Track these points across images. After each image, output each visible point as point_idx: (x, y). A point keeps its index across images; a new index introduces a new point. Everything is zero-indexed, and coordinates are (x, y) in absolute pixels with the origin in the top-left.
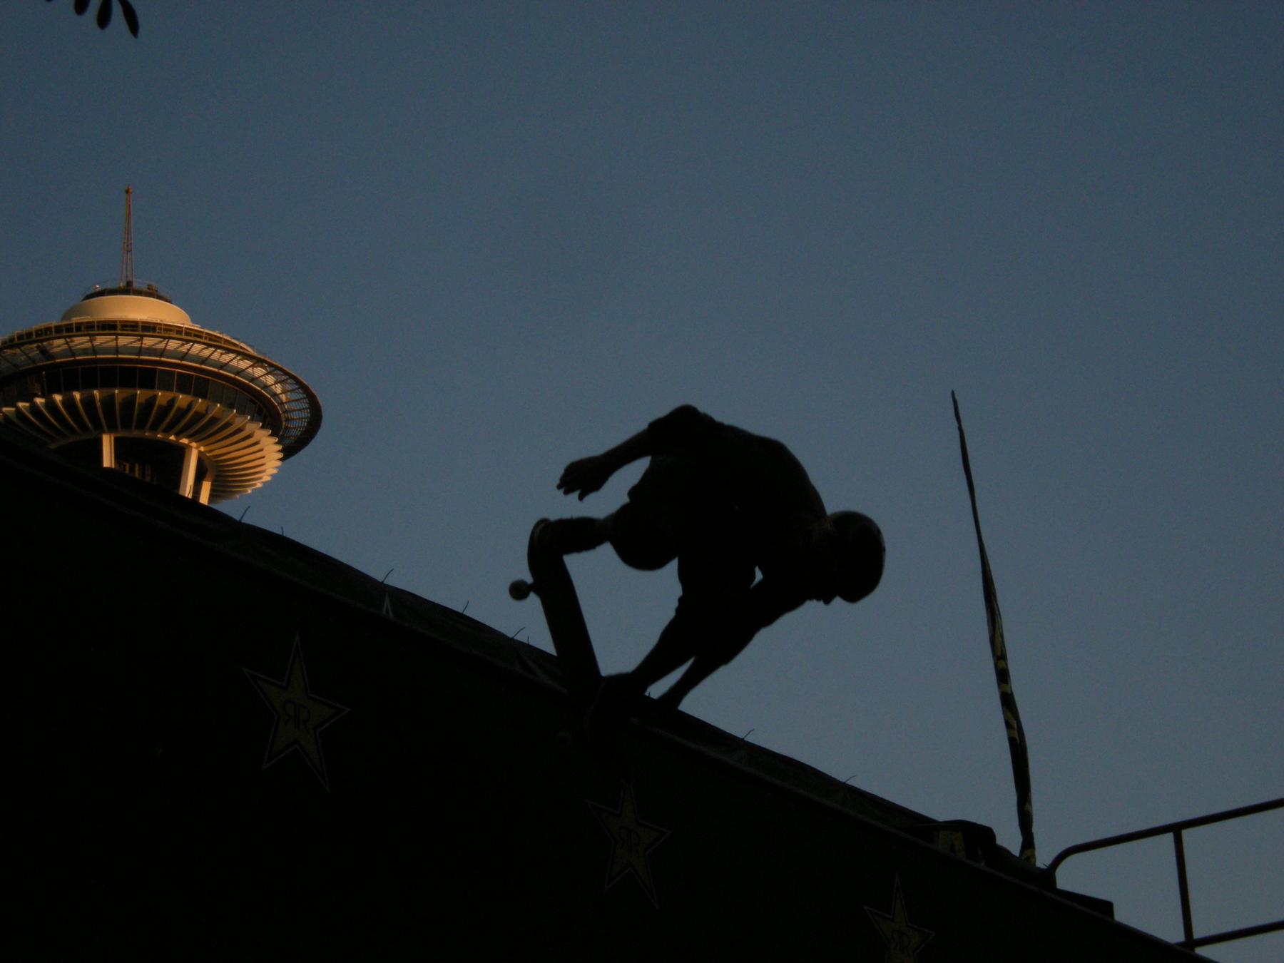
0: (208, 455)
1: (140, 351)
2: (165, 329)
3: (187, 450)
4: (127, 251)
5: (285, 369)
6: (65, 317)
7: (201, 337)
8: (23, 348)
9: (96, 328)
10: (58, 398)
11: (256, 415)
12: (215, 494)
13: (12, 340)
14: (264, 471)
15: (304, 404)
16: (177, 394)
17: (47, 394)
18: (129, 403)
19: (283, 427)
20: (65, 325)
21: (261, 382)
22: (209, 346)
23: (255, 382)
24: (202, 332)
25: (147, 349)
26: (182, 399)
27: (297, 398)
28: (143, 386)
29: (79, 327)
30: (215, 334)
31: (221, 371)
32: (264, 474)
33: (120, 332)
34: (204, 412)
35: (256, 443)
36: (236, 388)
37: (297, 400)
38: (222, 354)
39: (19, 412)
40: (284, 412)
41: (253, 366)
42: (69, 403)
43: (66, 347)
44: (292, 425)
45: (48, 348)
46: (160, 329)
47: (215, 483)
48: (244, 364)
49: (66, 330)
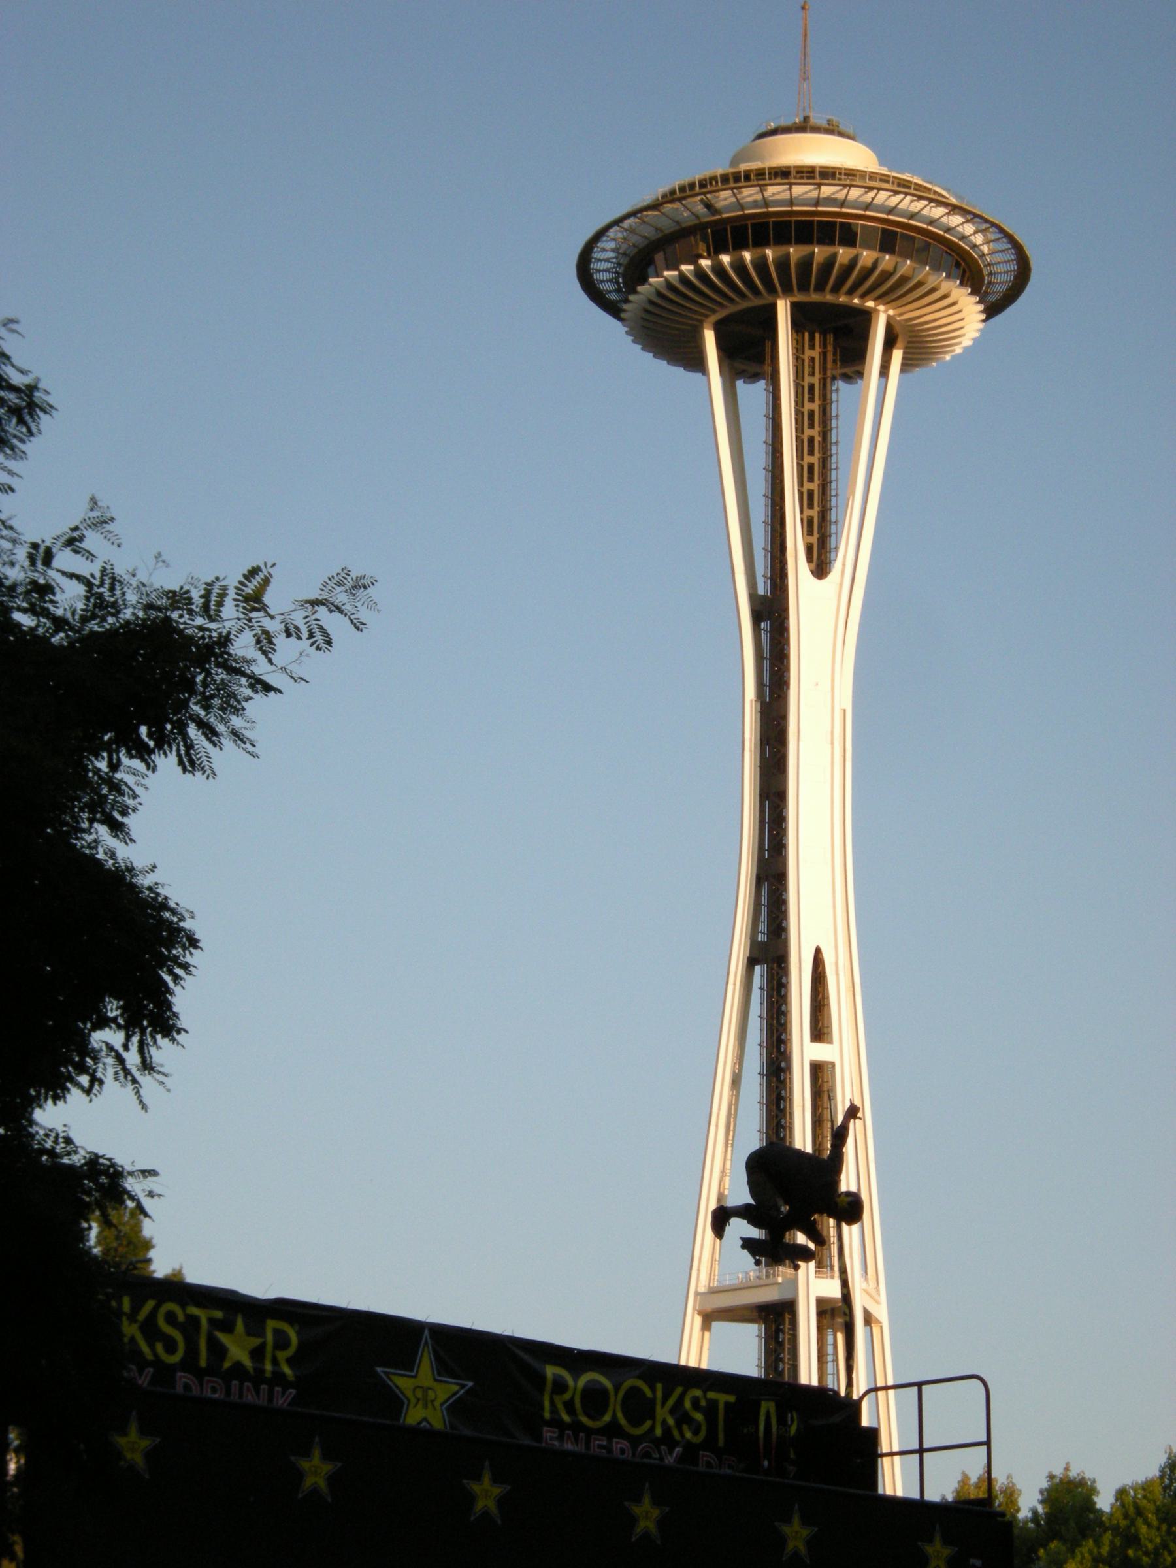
0: (898, 319)
1: (817, 202)
3: (873, 315)
4: (804, 80)
6: (735, 161)
7: (887, 182)
8: (684, 202)
9: (767, 177)
10: (725, 259)
11: (953, 267)
13: (673, 192)
15: (1011, 256)
16: (860, 250)
17: (714, 253)
18: (806, 264)
19: (986, 282)
20: (733, 174)
21: (959, 232)
22: (896, 193)
23: (952, 232)
26: (867, 256)
27: (1003, 248)
28: (821, 242)
29: (747, 177)
31: (911, 222)
33: (793, 181)
34: (890, 268)
35: (954, 304)
38: (912, 201)
39: (683, 278)
40: (984, 266)
41: (948, 214)
42: (739, 266)
43: (733, 199)
44: (998, 279)
45: (713, 202)
46: (840, 174)
47: (908, 350)
48: (938, 212)
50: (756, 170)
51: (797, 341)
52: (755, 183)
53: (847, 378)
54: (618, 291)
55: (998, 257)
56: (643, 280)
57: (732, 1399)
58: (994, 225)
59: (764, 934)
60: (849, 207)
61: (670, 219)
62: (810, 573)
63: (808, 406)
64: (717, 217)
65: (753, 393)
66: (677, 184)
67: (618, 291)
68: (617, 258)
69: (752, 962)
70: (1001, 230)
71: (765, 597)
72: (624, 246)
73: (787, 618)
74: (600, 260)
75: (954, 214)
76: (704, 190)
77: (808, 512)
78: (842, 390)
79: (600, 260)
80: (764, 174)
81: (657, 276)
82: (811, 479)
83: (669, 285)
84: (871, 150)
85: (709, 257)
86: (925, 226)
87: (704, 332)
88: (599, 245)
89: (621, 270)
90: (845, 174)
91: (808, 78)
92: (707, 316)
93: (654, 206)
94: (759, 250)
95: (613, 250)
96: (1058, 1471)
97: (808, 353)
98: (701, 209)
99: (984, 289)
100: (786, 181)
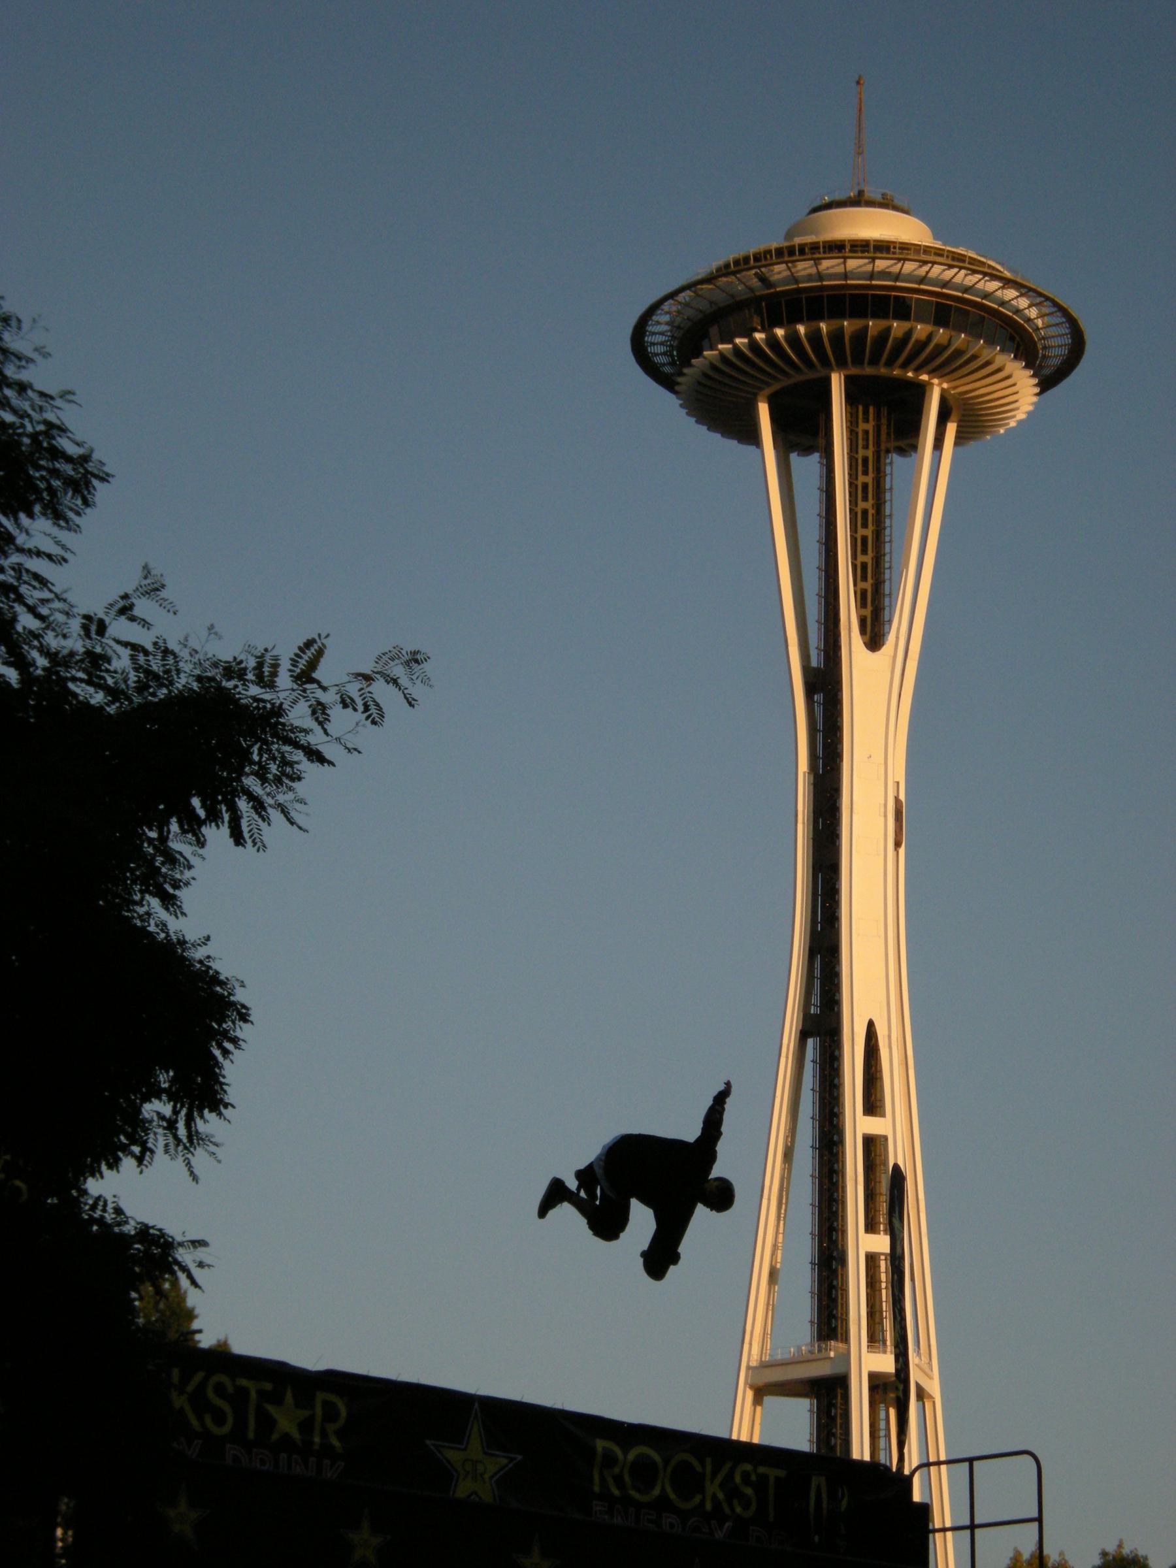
0: (952, 392)
1: (872, 275)
2: (900, 248)
3: (927, 388)
5: (1040, 290)
6: (789, 235)
7: (942, 255)
8: (738, 276)
9: (821, 250)
12: (962, 435)
13: (727, 266)
14: (1017, 409)
15: (1065, 330)
16: (914, 324)
17: (767, 328)
18: (860, 336)
19: (1040, 355)
20: (788, 247)
21: (1012, 305)
22: (951, 267)
23: (1007, 306)
24: (943, 250)
25: (879, 272)
26: (921, 330)
27: (1058, 322)
28: (875, 316)
29: (802, 249)
30: (959, 251)
31: (966, 296)
32: (1019, 411)
33: (847, 255)
34: (944, 341)
36: (982, 314)
37: (1057, 324)
38: (966, 275)
39: (737, 350)
40: (1040, 339)
41: (1003, 288)
42: (793, 339)
43: (788, 273)
45: (767, 275)
46: (895, 248)
47: (962, 424)
48: (992, 286)
49: (788, 253)
50: (811, 243)
51: (851, 417)
52: (809, 256)
53: (902, 451)
54: (672, 364)
55: (1053, 331)
56: (698, 353)
57: (781, 1473)
58: (1047, 298)
59: (817, 1007)
60: (903, 281)
61: (723, 291)
62: (863, 645)
63: (862, 479)
64: (772, 290)
65: (806, 466)
66: (731, 258)
67: (672, 364)
68: (671, 331)
69: (804, 1035)
70: (1055, 304)
71: (817, 671)
72: (679, 319)
73: (840, 690)
74: (654, 334)
75: (1009, 288)
76: (757, 264)
77: (861, 585)
78: (897, 463)
79: (654, 334)
80: (819, 248)
81: (712, 348)
82: (864, 552)
83: (723, 357)
84: (925, 223)
85: (763, 330)
86: (979, 300)
87: (758, 405)
88: (654, 318)
89: (675, 343)
90: (900, 248)
91: (862, 153)
92: (761, 389)
93: (709, 279)
94: (814, 324)
95: (667, 323)
96: (1111, 1548)
97: (862, 426)
98: (755, 283)
99: (1038, 362)
100: (840, 255)
